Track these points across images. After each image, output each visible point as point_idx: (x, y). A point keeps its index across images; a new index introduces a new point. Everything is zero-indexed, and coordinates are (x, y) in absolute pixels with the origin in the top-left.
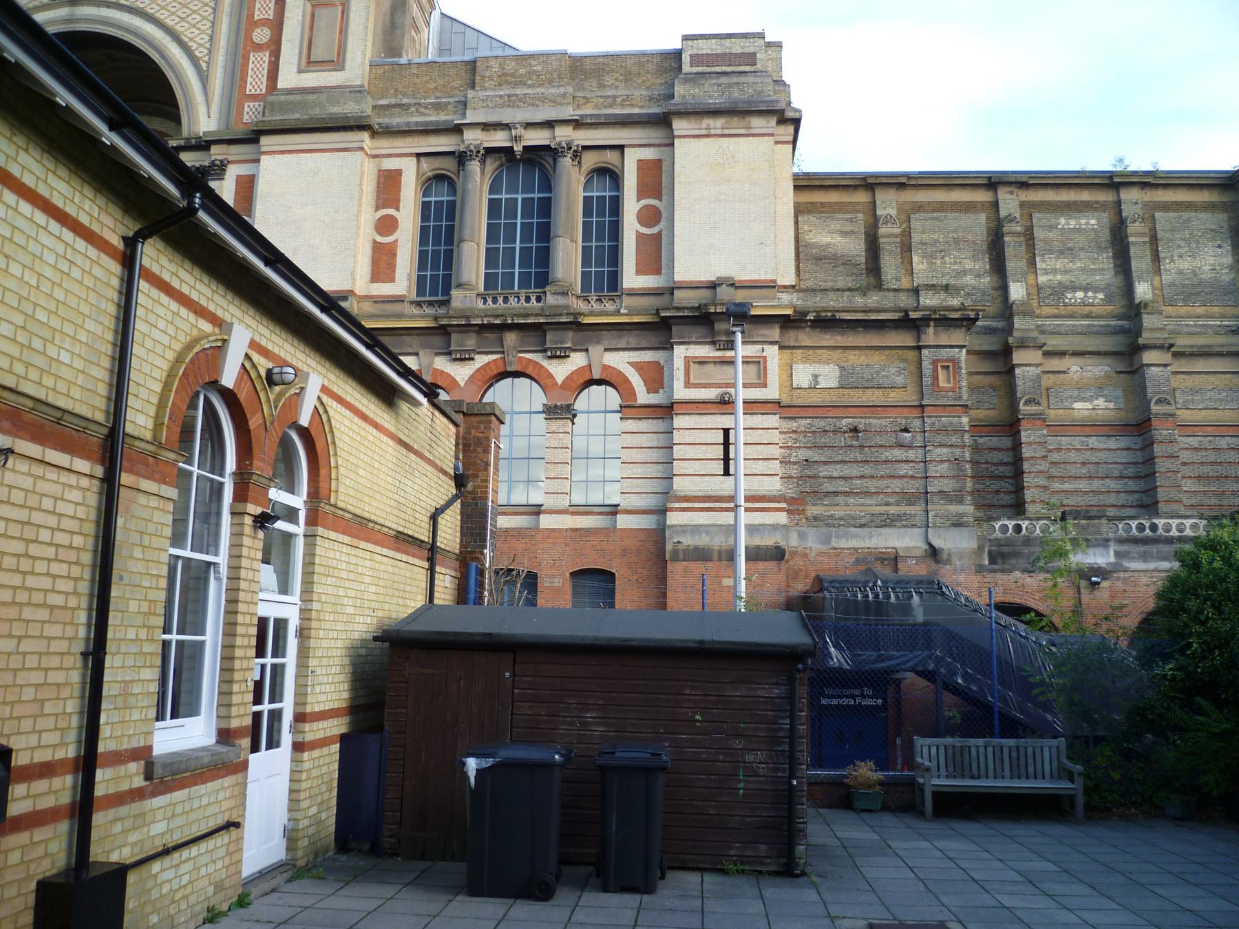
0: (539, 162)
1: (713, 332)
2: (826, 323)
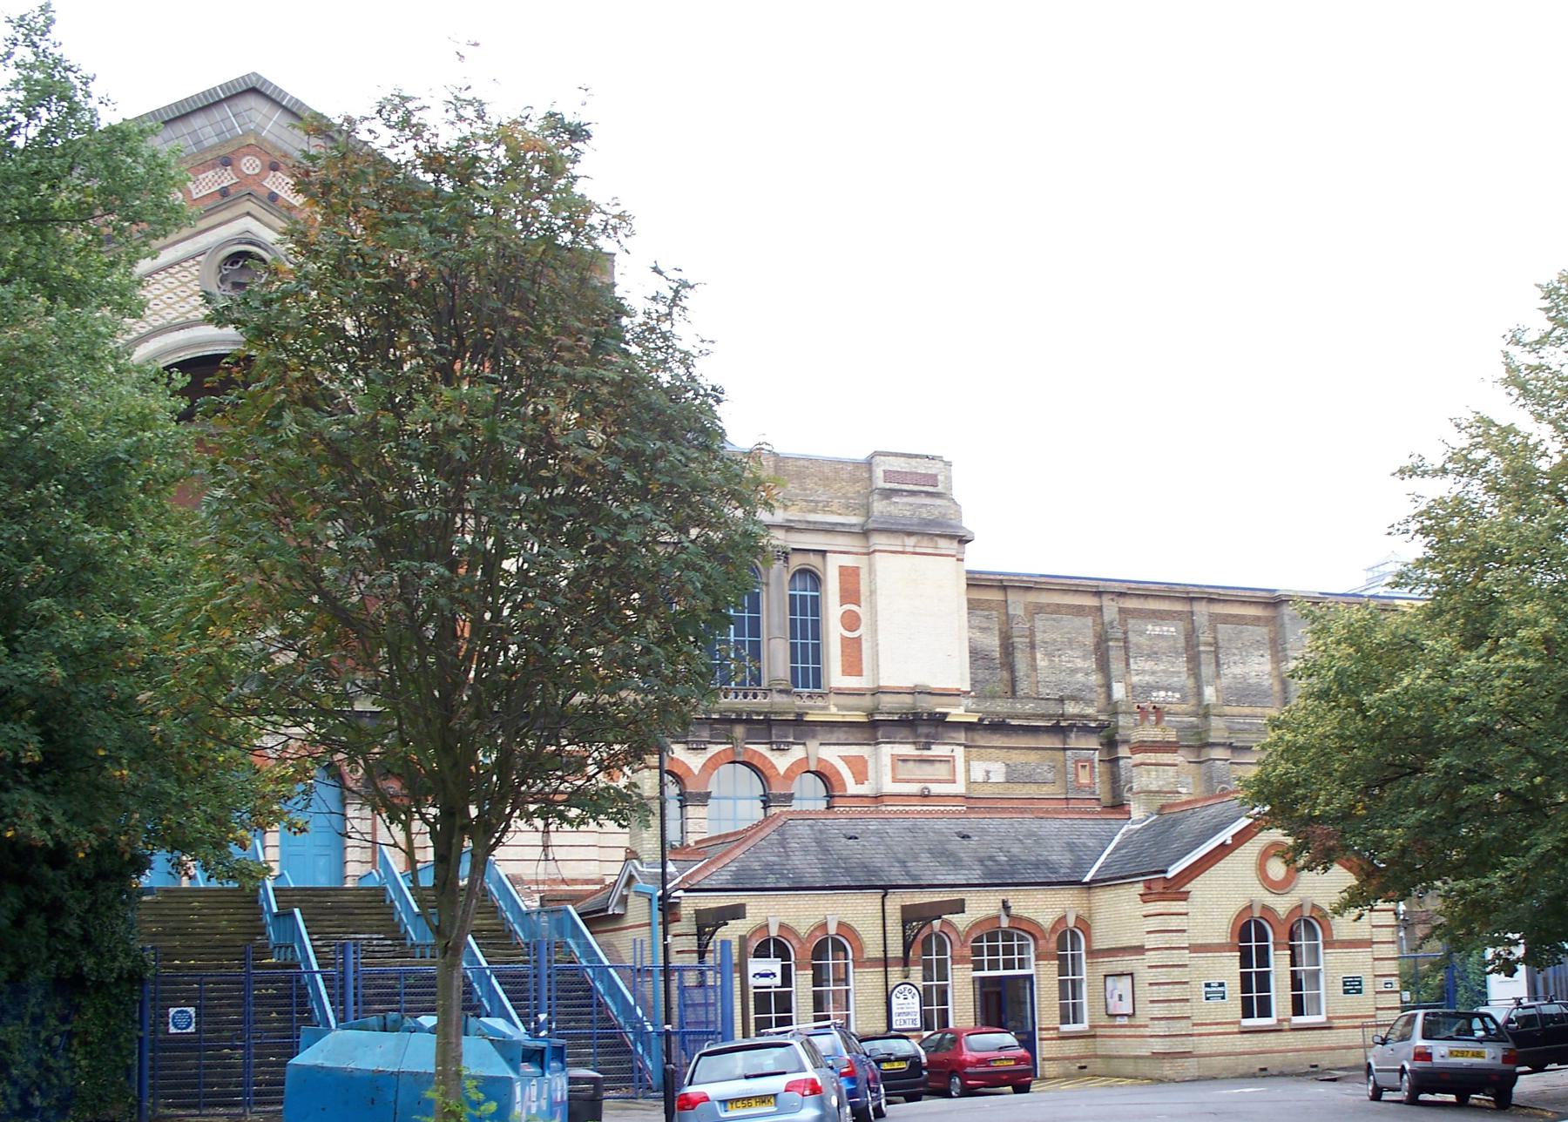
2: (998, 726)
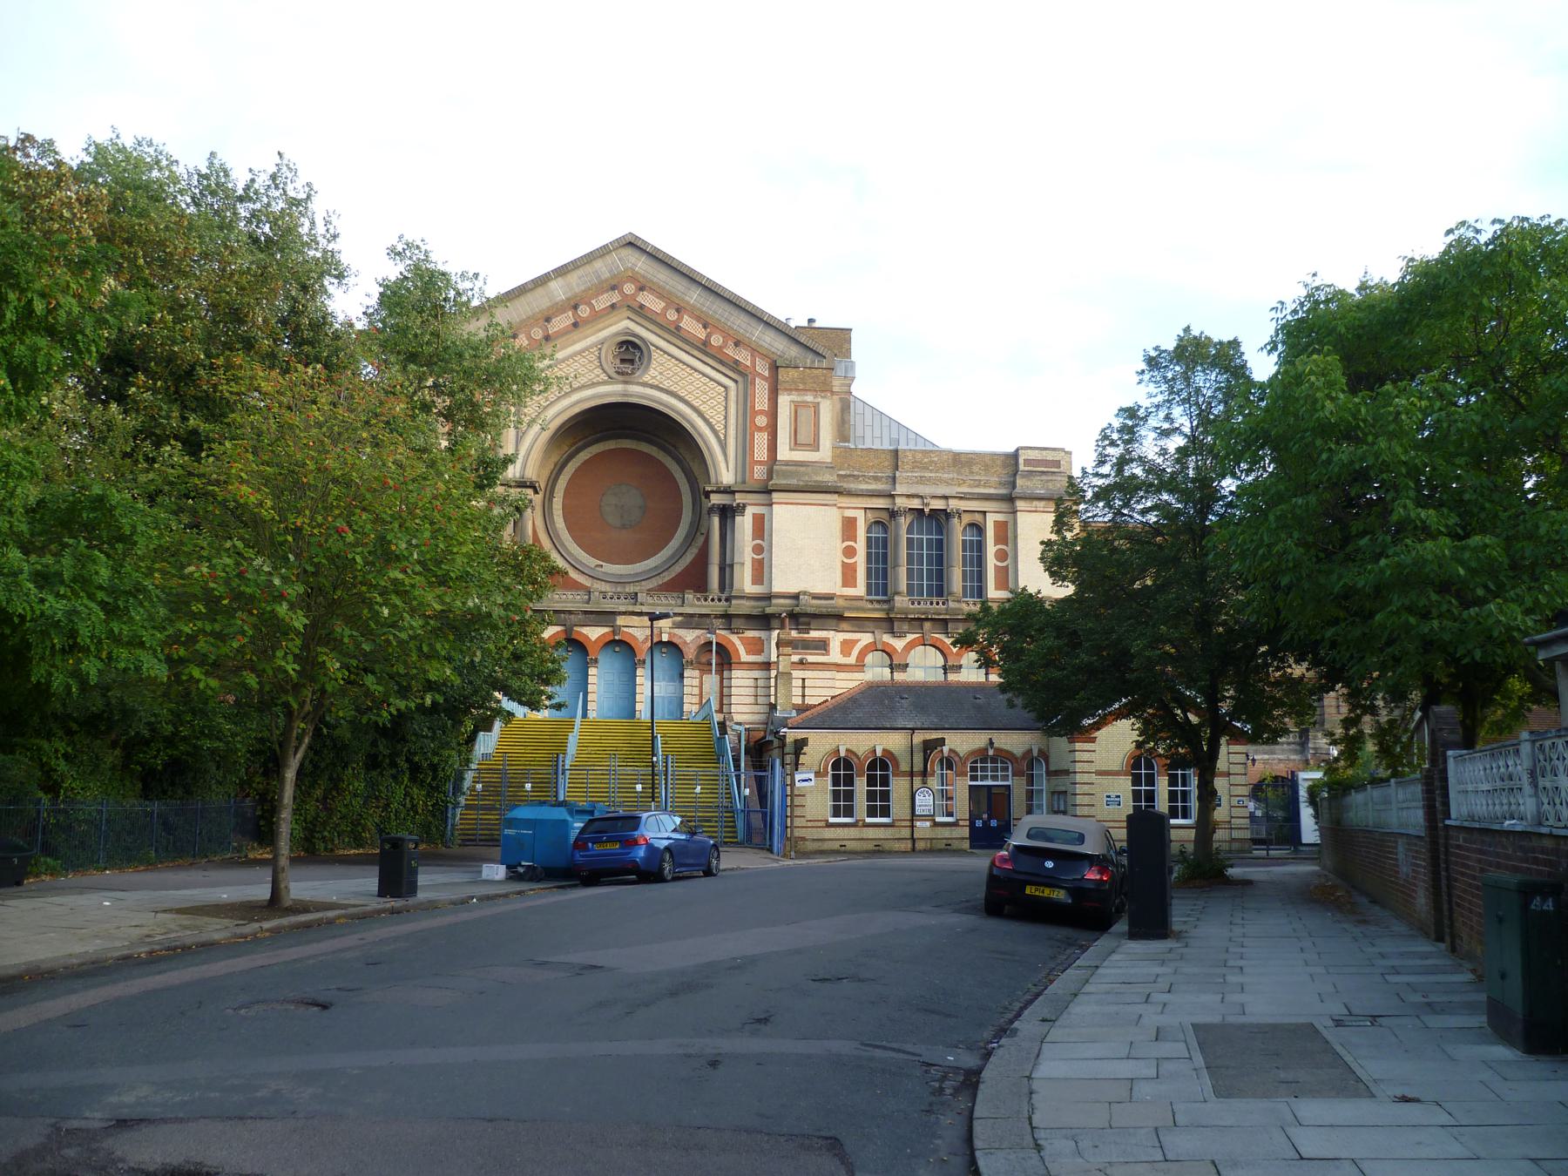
0: (938, 520)
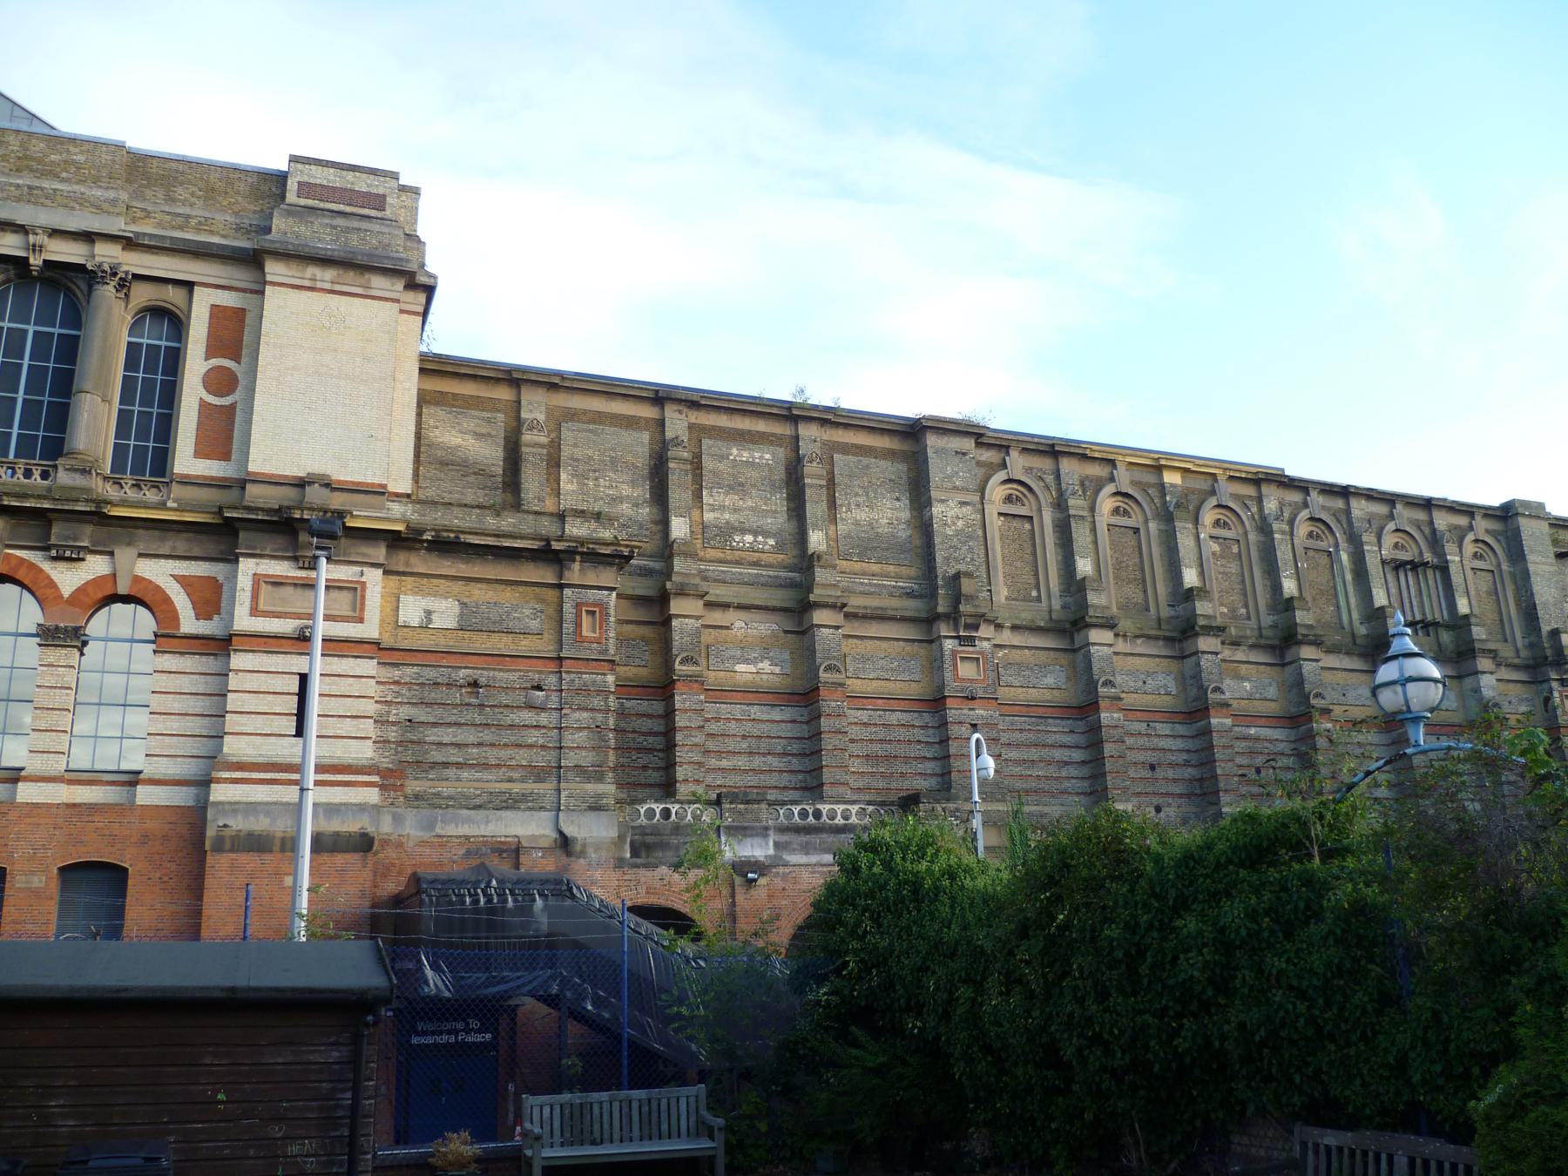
1: (295, 545)
2: (447, 546)
